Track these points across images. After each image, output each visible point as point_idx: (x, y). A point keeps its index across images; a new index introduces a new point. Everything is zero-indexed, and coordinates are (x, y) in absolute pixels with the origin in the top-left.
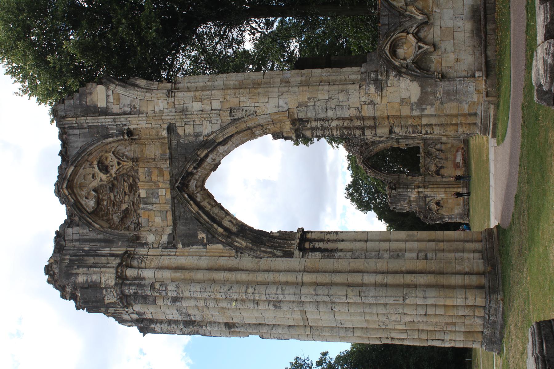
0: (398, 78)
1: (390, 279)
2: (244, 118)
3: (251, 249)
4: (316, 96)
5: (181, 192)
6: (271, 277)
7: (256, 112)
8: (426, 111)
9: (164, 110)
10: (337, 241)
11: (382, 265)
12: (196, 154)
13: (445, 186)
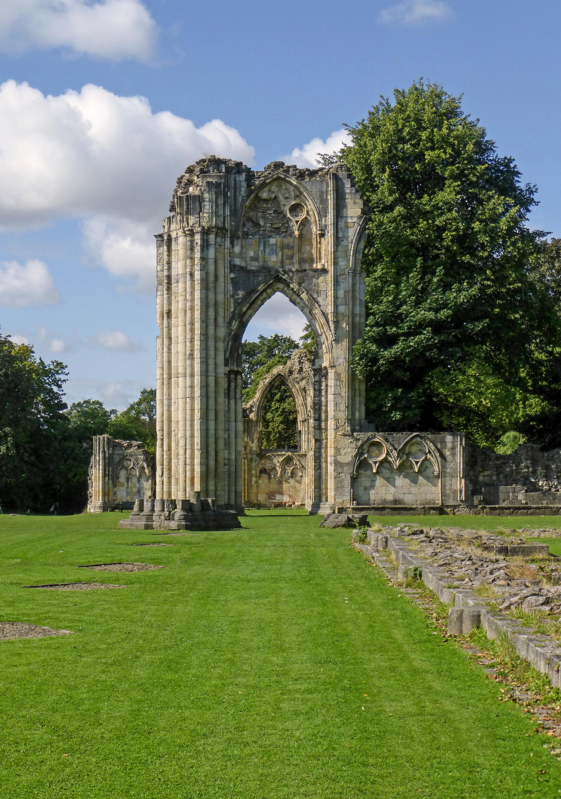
1: (212, 440)
3: (230, 334)
5: (275, 277)
6: (212, 353)
10: (236, 399)
11: (221, 434)
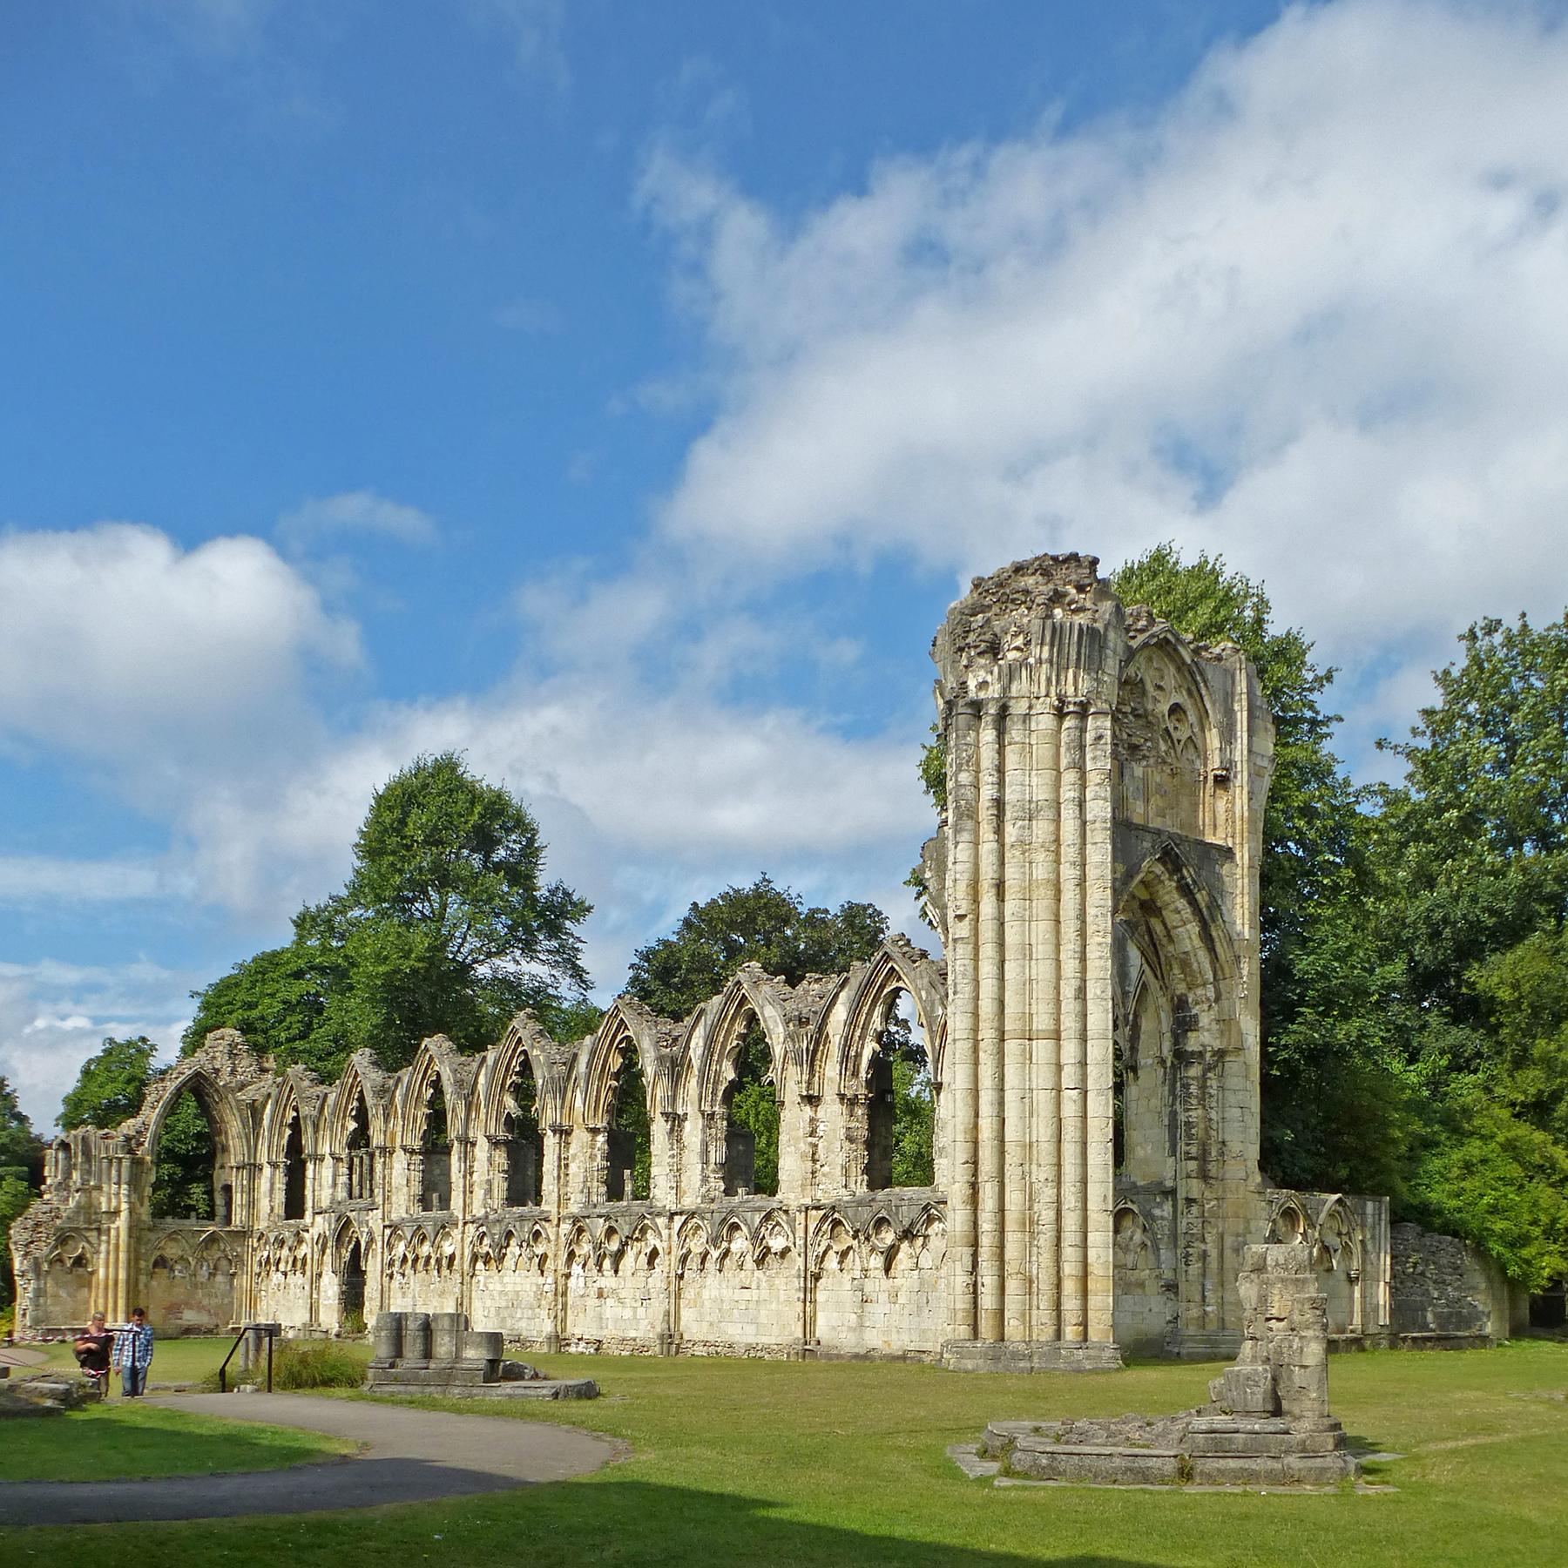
13: (131, 1281)
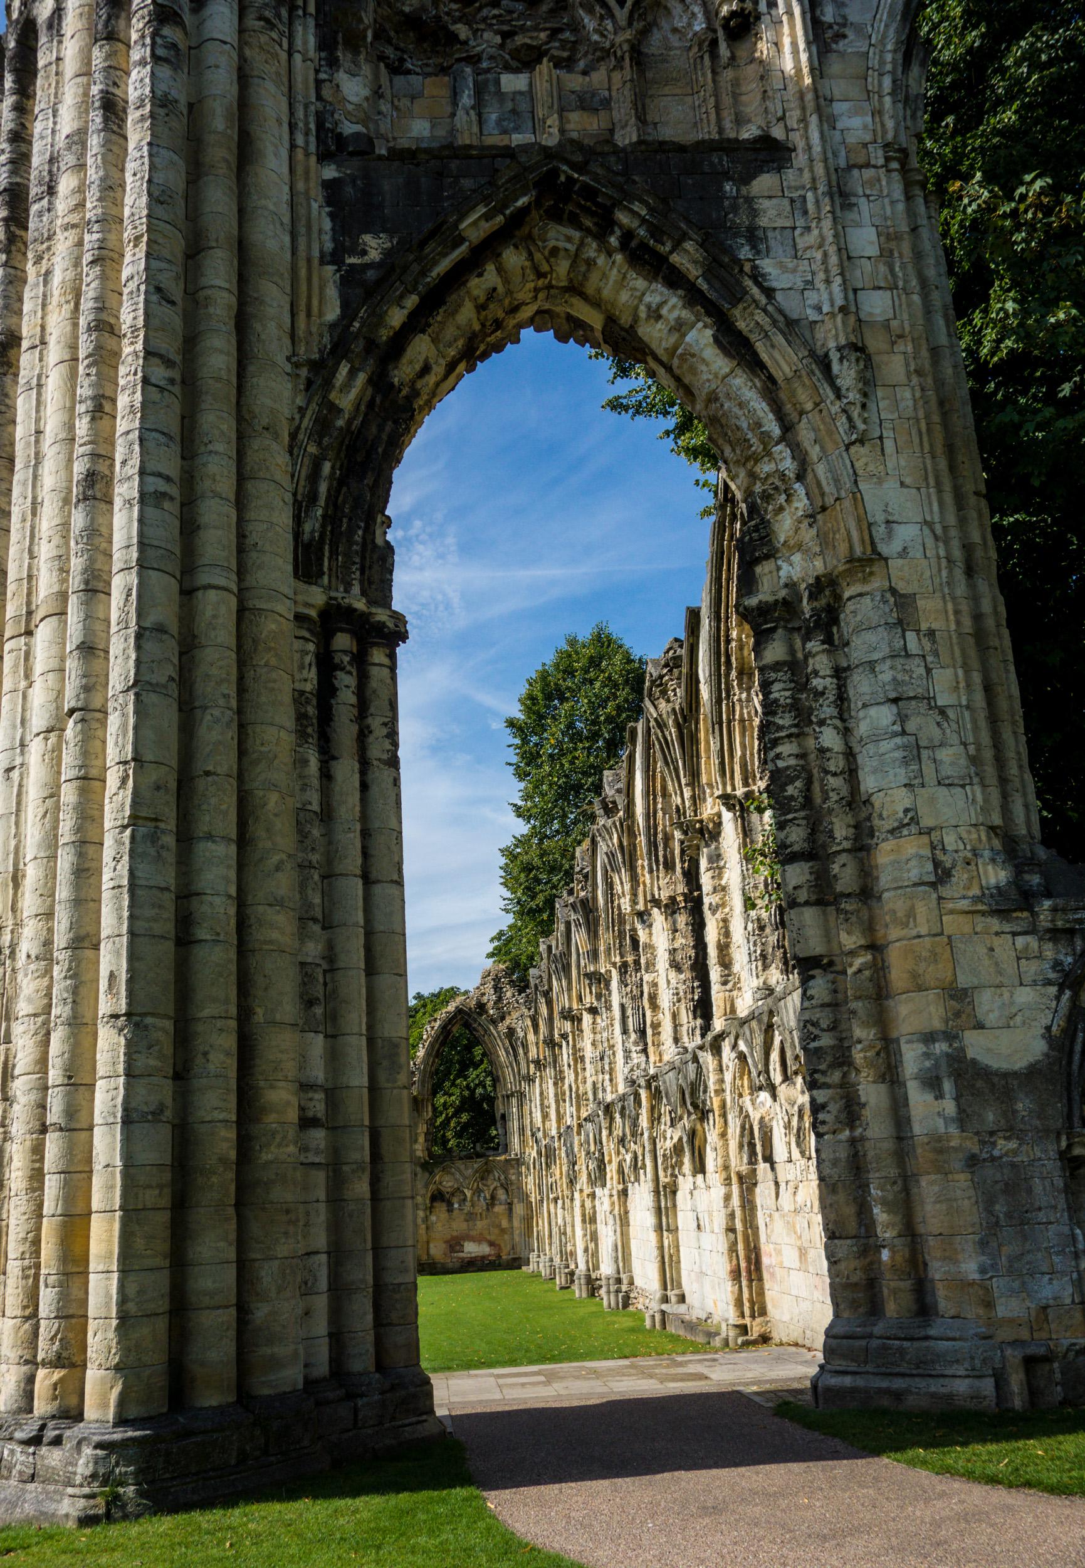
0: (1052, 975)
2: (839, 396)
3: (322, 426)
4: (945, 658)
5: (536, 185)
7: (861, 441)
8: (929, 1097)
9: (838, 133)
10: (365, 764)
12: (684, 237)
